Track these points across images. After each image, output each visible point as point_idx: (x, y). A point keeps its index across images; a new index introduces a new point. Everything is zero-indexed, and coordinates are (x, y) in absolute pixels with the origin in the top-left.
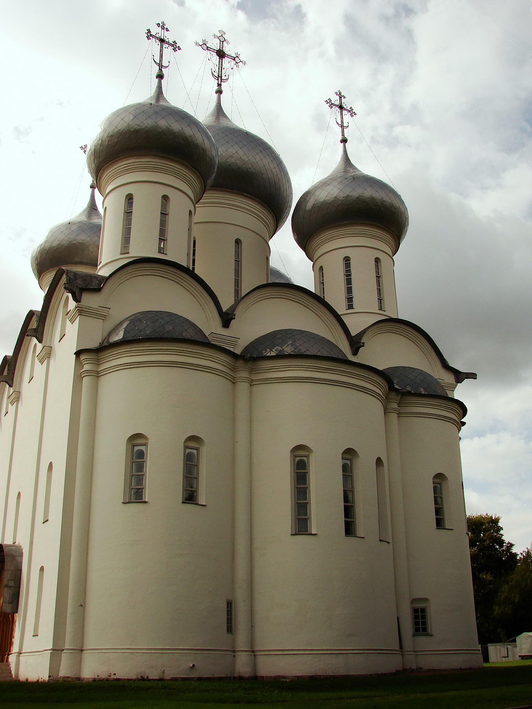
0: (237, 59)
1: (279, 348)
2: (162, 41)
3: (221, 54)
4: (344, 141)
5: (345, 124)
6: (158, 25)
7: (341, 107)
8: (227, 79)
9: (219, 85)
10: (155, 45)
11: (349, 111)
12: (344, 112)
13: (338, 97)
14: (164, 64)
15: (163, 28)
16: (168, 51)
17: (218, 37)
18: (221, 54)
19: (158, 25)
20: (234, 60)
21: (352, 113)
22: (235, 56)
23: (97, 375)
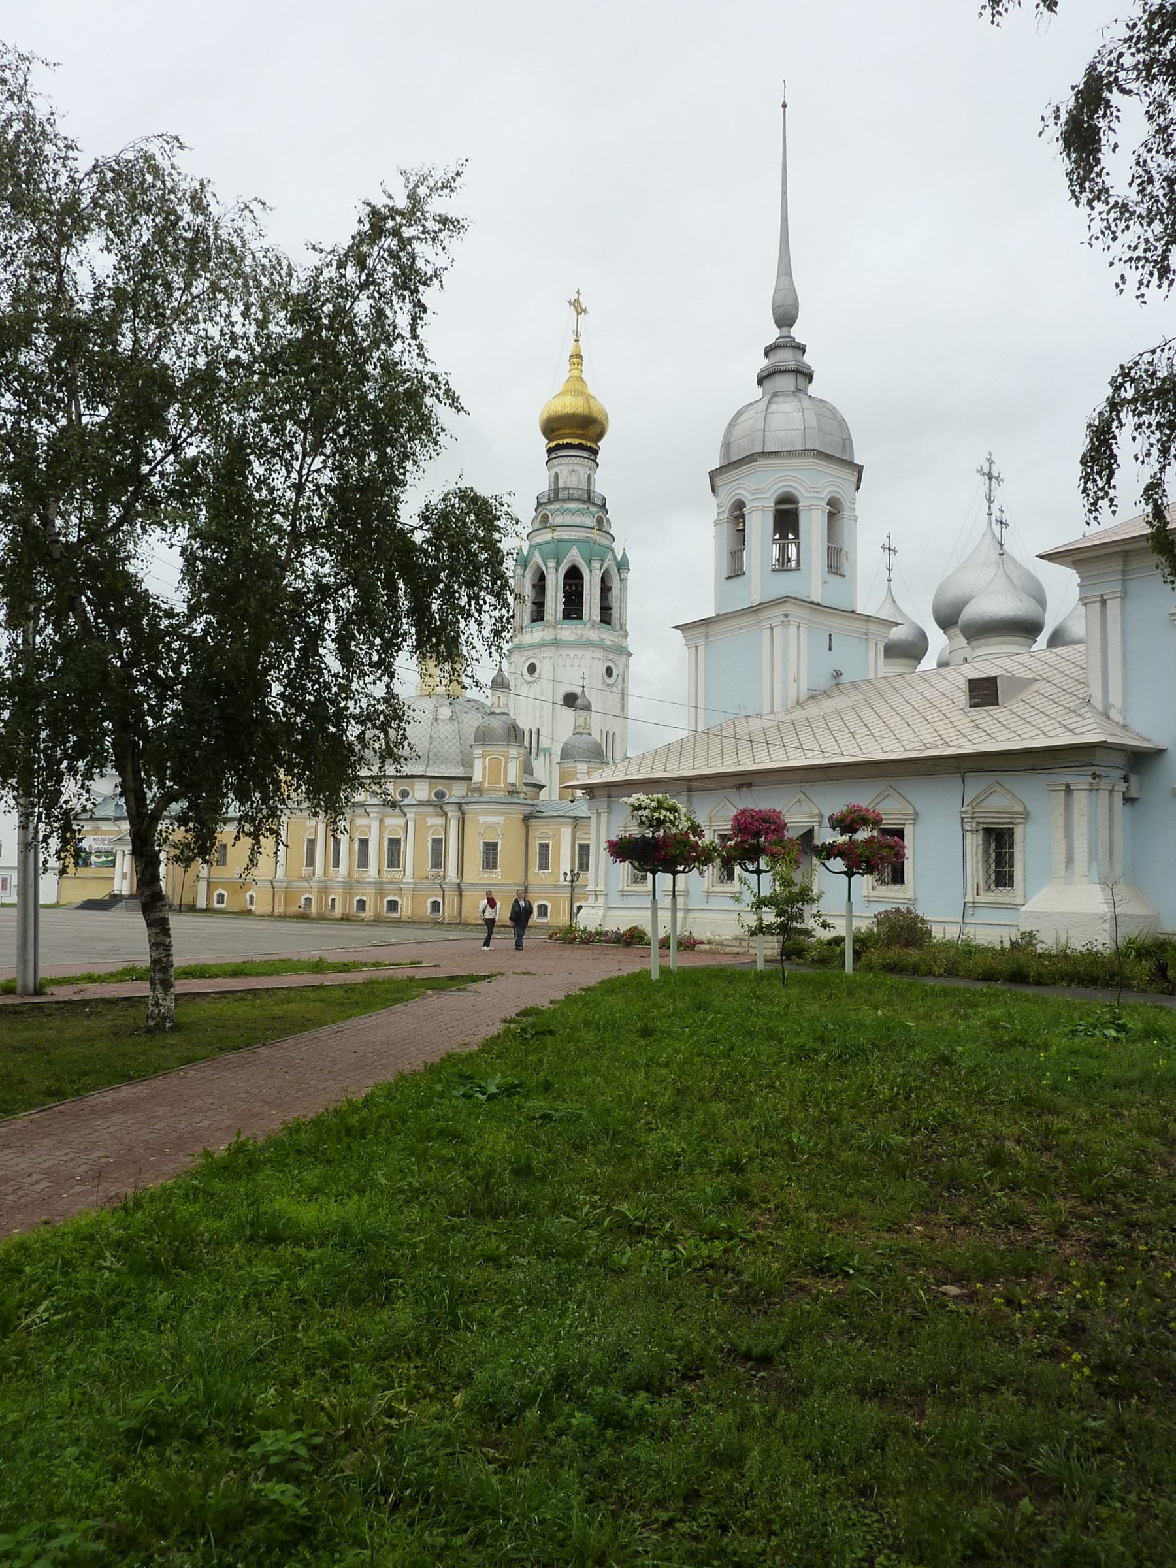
3: (990, 477)
18: (990, 477)
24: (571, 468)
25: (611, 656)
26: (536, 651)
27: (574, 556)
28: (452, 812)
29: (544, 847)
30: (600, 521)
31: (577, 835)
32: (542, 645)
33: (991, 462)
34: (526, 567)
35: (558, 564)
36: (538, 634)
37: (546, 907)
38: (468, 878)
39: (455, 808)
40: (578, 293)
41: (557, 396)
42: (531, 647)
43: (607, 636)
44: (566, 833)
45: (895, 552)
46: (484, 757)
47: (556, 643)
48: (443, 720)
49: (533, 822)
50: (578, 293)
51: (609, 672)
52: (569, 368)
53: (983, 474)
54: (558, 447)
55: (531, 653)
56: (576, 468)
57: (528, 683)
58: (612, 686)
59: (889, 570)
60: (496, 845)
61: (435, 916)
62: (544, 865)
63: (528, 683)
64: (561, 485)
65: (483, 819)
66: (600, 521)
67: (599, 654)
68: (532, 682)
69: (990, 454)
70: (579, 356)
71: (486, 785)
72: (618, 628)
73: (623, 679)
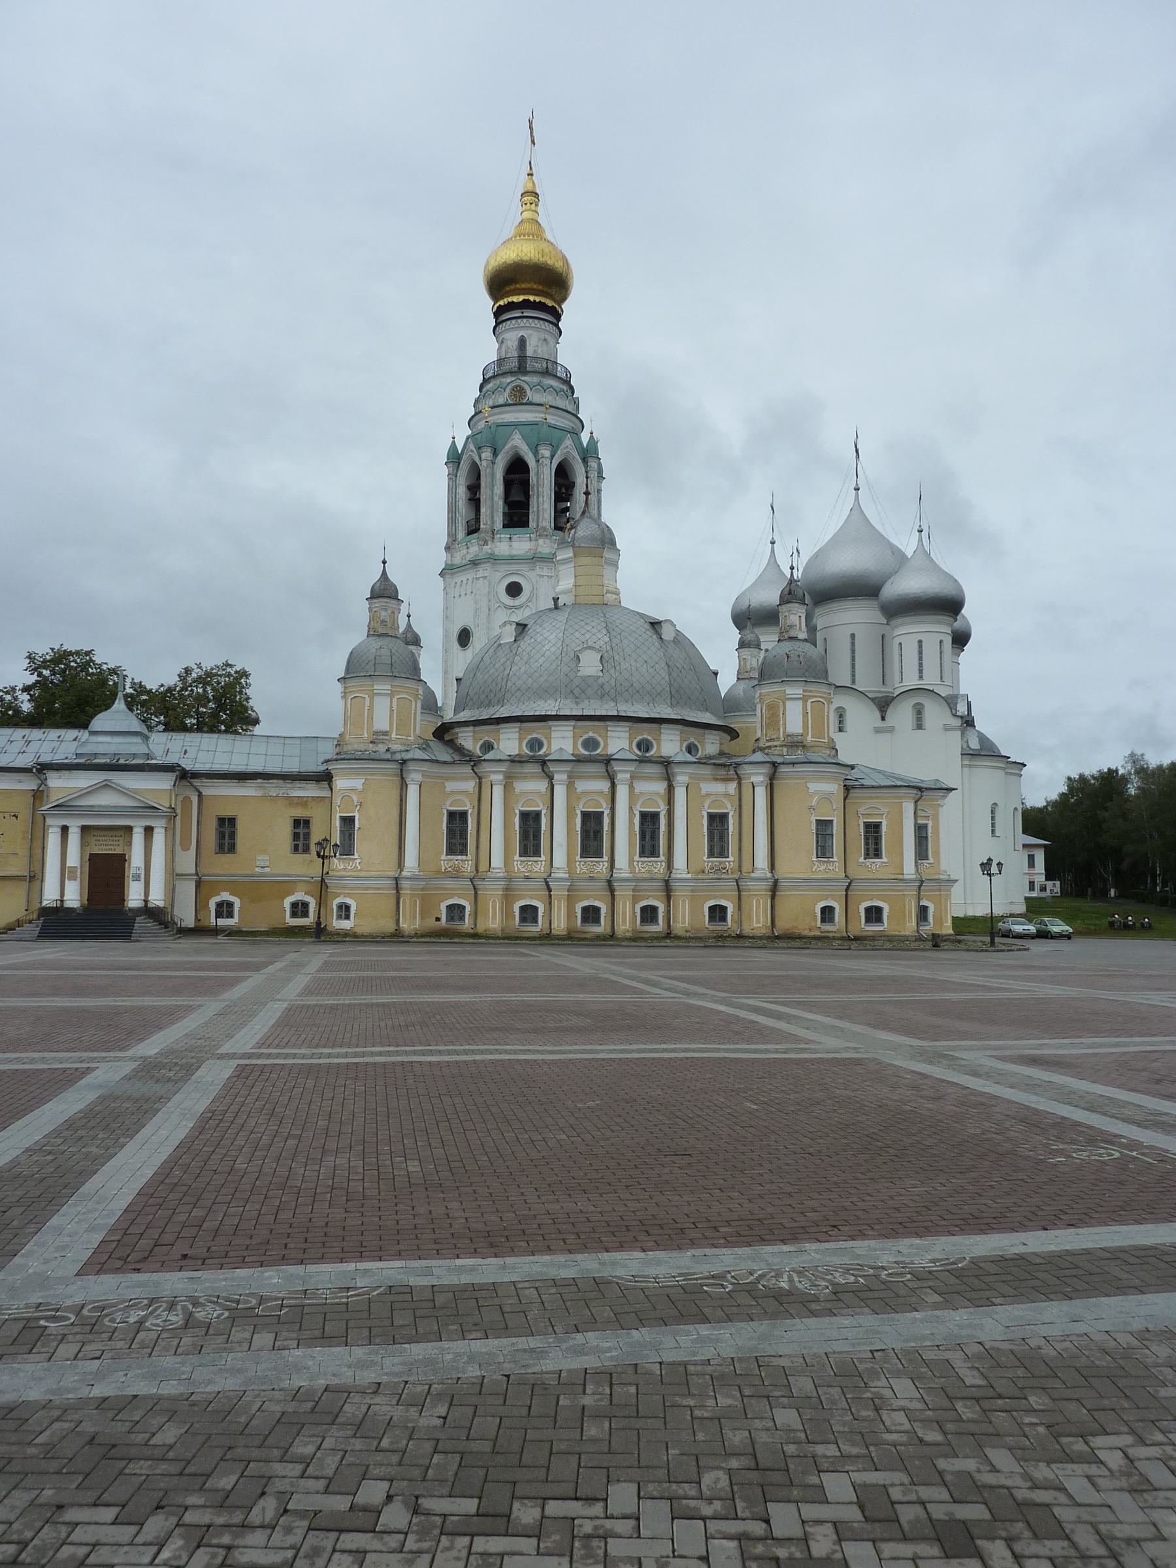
23: (970, 766)
26: (524, 568)
28: (758, 777)
29: (873, 830)
32: (534, 559)
34: (495, 453)
36: (520, 544)
37: (879, 910)
38: (782, 870)
39: (766, 770)
42: (512, 559)
44: (908, 808)
46: (804, 699)
48: (669, 642)
55: (514, 568)
57: (508, 607)
61: (718, 927)
62: (873, 848)
63: (508, 607)
64: (529, 352)
65: (813, 786)
68: (517, 608)
70: (536, 195)
71: (809, 738)
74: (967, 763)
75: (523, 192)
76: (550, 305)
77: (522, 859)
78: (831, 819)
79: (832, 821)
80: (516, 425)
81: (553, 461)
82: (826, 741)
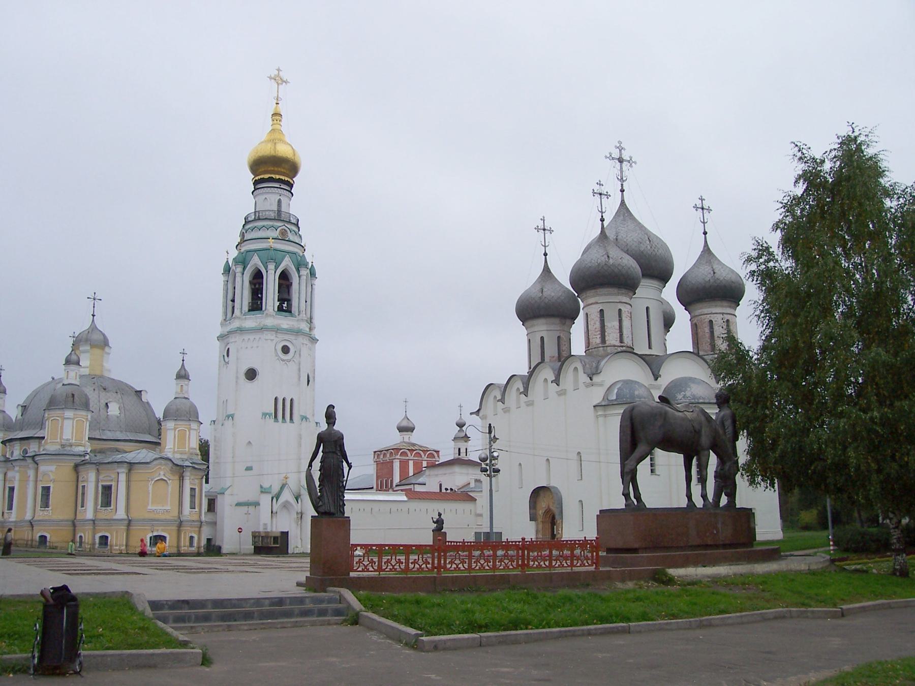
0: (631, 161)
1: (684, 393)
2: (601, 194)
3: (621, 160)
4: (705, 233)
5: (706, 221)
6: (597, 183)
7: (703, 209)
8: (626, 180)
9: (622, 185)
10: (597, 196)
11: (707, 209)
12: (705, 211)
13: (700, 201)
14: (604, 211)
15: (600, 185)
16: (604, 198)
17: (618, 147)
18: (621, 160)
19: (597, 183)
20: (629, 162)
21: (709, 210)
22: (629, 159)
23: (605, 416)
24: (264, 197)
25: (286, 337)
27: (256, 261)
30: (283, 233)
31: (101, 477)
33: (621, 149)
35: (244, 269)
40: (279, 70)
41: (262, 142)
43: (285, 322)
45: (551, 231)
47: (241, 330)
49: (81, 468)
50: (279, 70)
51: (286, 350)
52: (271, 123)
53: (613, 159)
54: (263, 181)
56: (266, 196)
58: (289, 361)
59: (545, 246)
60: (48, 488)
66: (283, 233)
67: (270, 336)
69: (620, 142)
72: (297, 314)
73: (300, 355)
74: (600, 413)
75: (273, 113)
76: (267, 177)
77: (8, 511)
78: (49, 485)
79: (50, 487)
80: (255, 251)
81: (245, 272)
82: (59, 440)
